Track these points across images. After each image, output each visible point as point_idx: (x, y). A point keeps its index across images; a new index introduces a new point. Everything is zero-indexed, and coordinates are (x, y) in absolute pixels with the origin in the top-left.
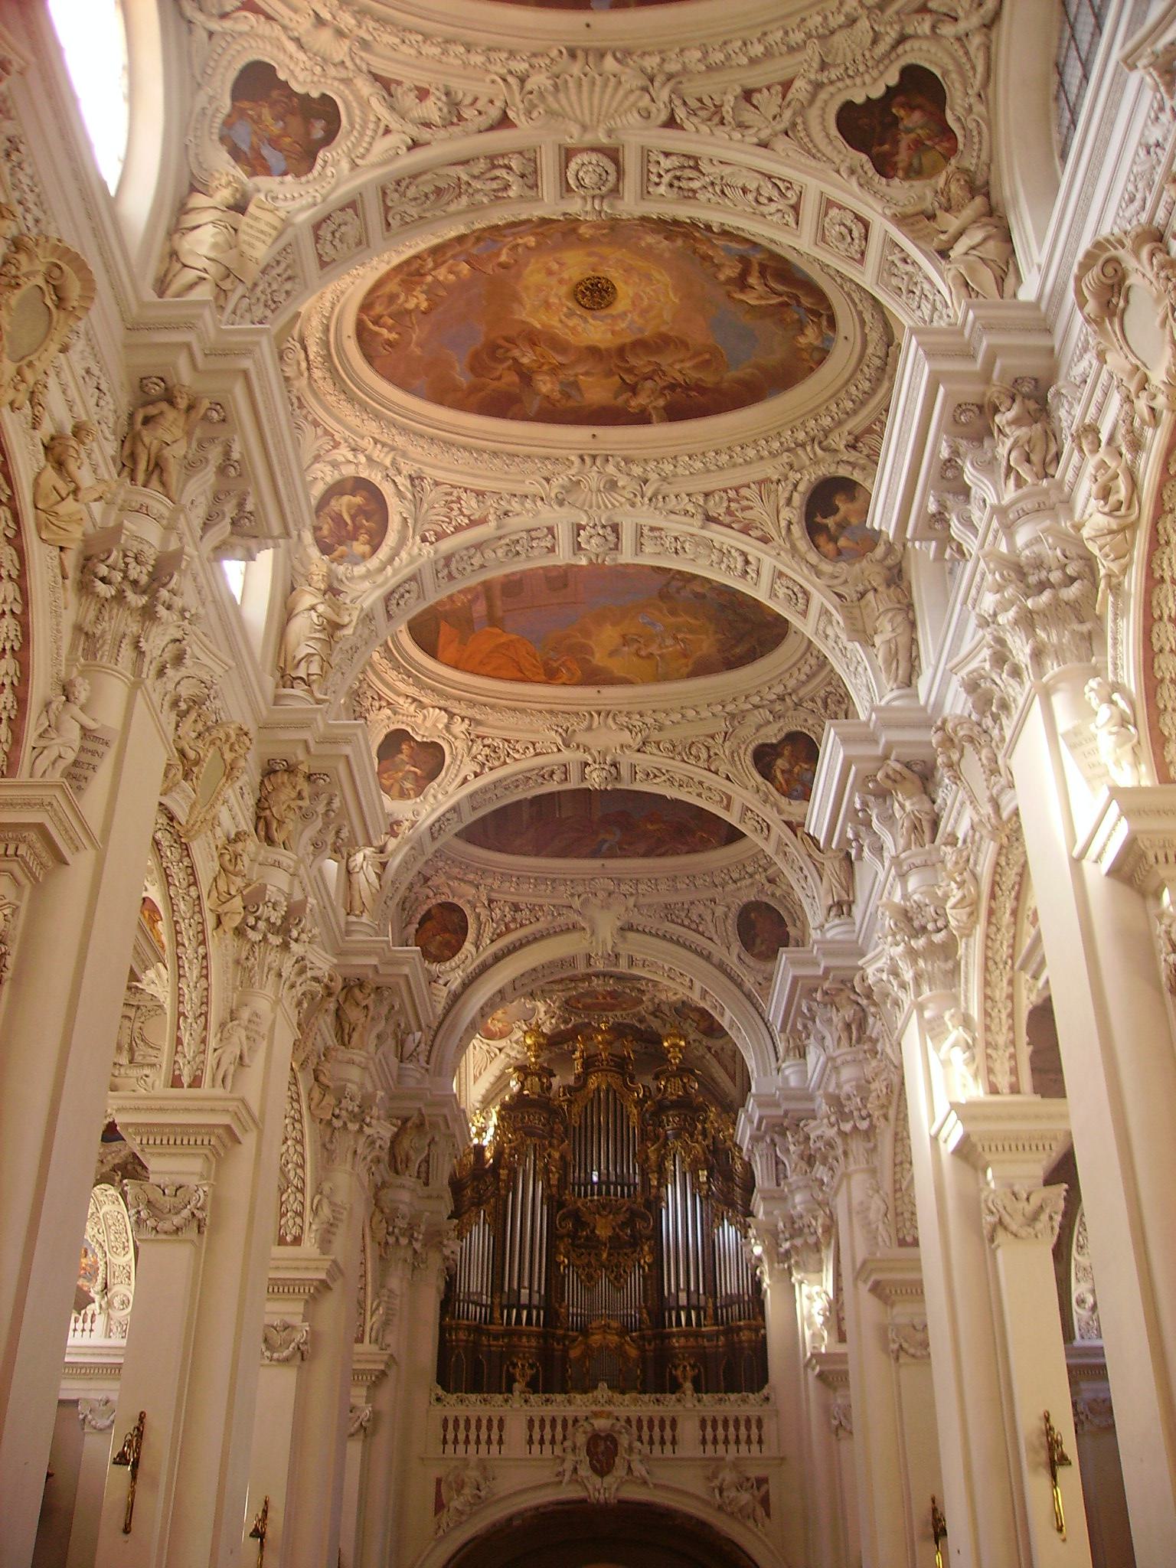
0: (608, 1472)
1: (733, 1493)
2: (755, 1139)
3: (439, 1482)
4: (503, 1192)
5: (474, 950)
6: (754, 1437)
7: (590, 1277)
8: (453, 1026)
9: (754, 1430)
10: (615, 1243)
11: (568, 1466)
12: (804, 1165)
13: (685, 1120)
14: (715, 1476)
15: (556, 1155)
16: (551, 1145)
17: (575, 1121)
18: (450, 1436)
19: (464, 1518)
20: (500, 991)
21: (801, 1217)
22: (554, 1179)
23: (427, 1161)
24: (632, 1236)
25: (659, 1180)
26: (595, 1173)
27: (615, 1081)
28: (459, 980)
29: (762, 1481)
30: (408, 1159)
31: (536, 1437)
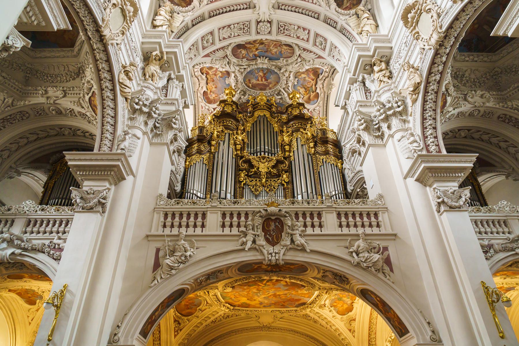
0: (277, 243)
1: (366, 255)
2: (353, 82)
3: (158, 250)
4: (213, 150)
5: (198, 4)
6: (374, 223)
7: (256, 190)
8: (186, 40)
9: (373, 219)
10: (269, 175)
11: (250, 238)
12: (386, 79)
13: (301, 125)
14: (352, 245)
15: (240, 138)
16: (237, 134)
17: (248, 129)
18: (168, 224)
19: (173, 272)
20: (211, 33)
21: (389, 102)
22: (239, 147)
23: (166, 88)
24: (279, 172)
25: (290, 149)
26: (258, 148)
27: (268, 114)
28: (189, 17)
29: (386, 249)
30: (152, 76)
31: (227, 224)
